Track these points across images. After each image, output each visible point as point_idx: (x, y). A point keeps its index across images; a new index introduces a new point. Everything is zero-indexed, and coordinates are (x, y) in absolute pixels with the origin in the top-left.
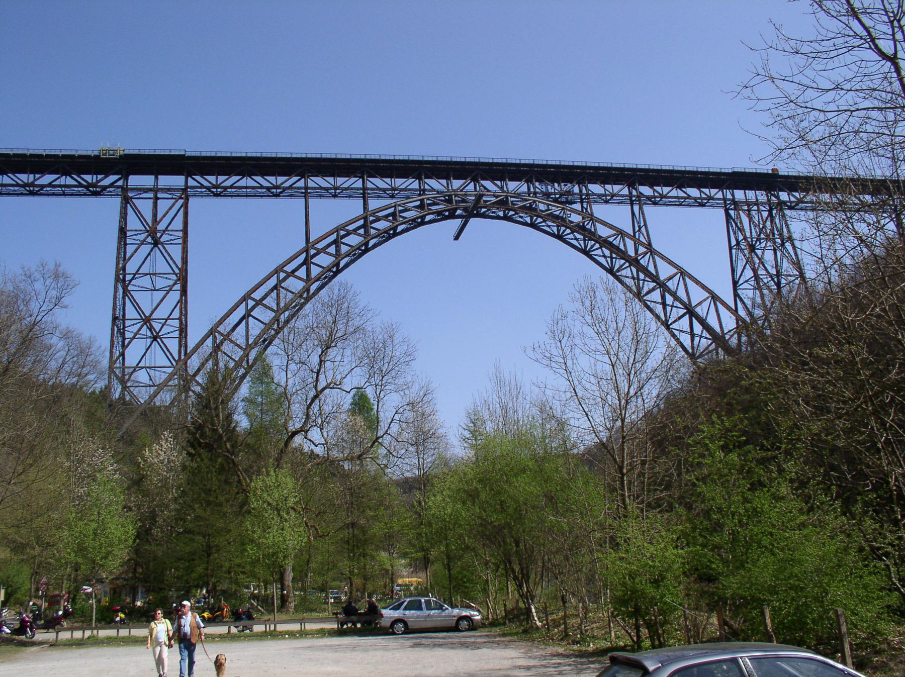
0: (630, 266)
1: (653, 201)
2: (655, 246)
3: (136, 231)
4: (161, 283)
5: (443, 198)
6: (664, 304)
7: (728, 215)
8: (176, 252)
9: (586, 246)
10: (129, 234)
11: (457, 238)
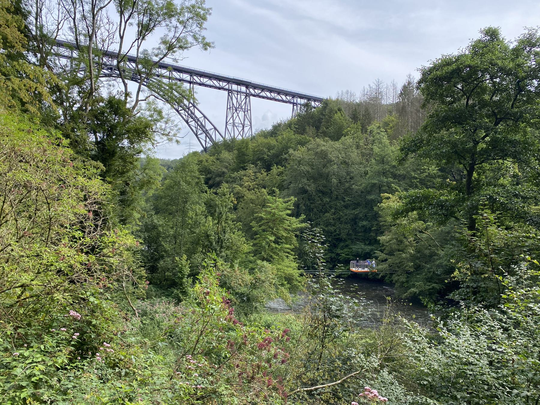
6: (206, 141)
7: (229, 95)
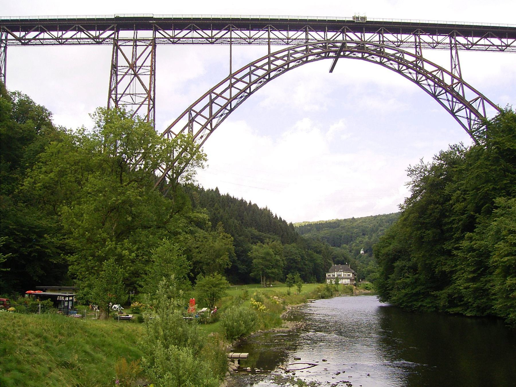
0: (445, 93)
1: (467, 48)
2: (464, 78)
3: (122, 66)
4: (139, 100)
5: (321, 45)
8: (146, 80)
9: (417, 78)
10: (119, 68)
11: (331, 71)
